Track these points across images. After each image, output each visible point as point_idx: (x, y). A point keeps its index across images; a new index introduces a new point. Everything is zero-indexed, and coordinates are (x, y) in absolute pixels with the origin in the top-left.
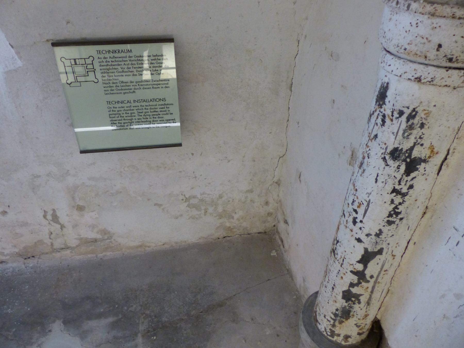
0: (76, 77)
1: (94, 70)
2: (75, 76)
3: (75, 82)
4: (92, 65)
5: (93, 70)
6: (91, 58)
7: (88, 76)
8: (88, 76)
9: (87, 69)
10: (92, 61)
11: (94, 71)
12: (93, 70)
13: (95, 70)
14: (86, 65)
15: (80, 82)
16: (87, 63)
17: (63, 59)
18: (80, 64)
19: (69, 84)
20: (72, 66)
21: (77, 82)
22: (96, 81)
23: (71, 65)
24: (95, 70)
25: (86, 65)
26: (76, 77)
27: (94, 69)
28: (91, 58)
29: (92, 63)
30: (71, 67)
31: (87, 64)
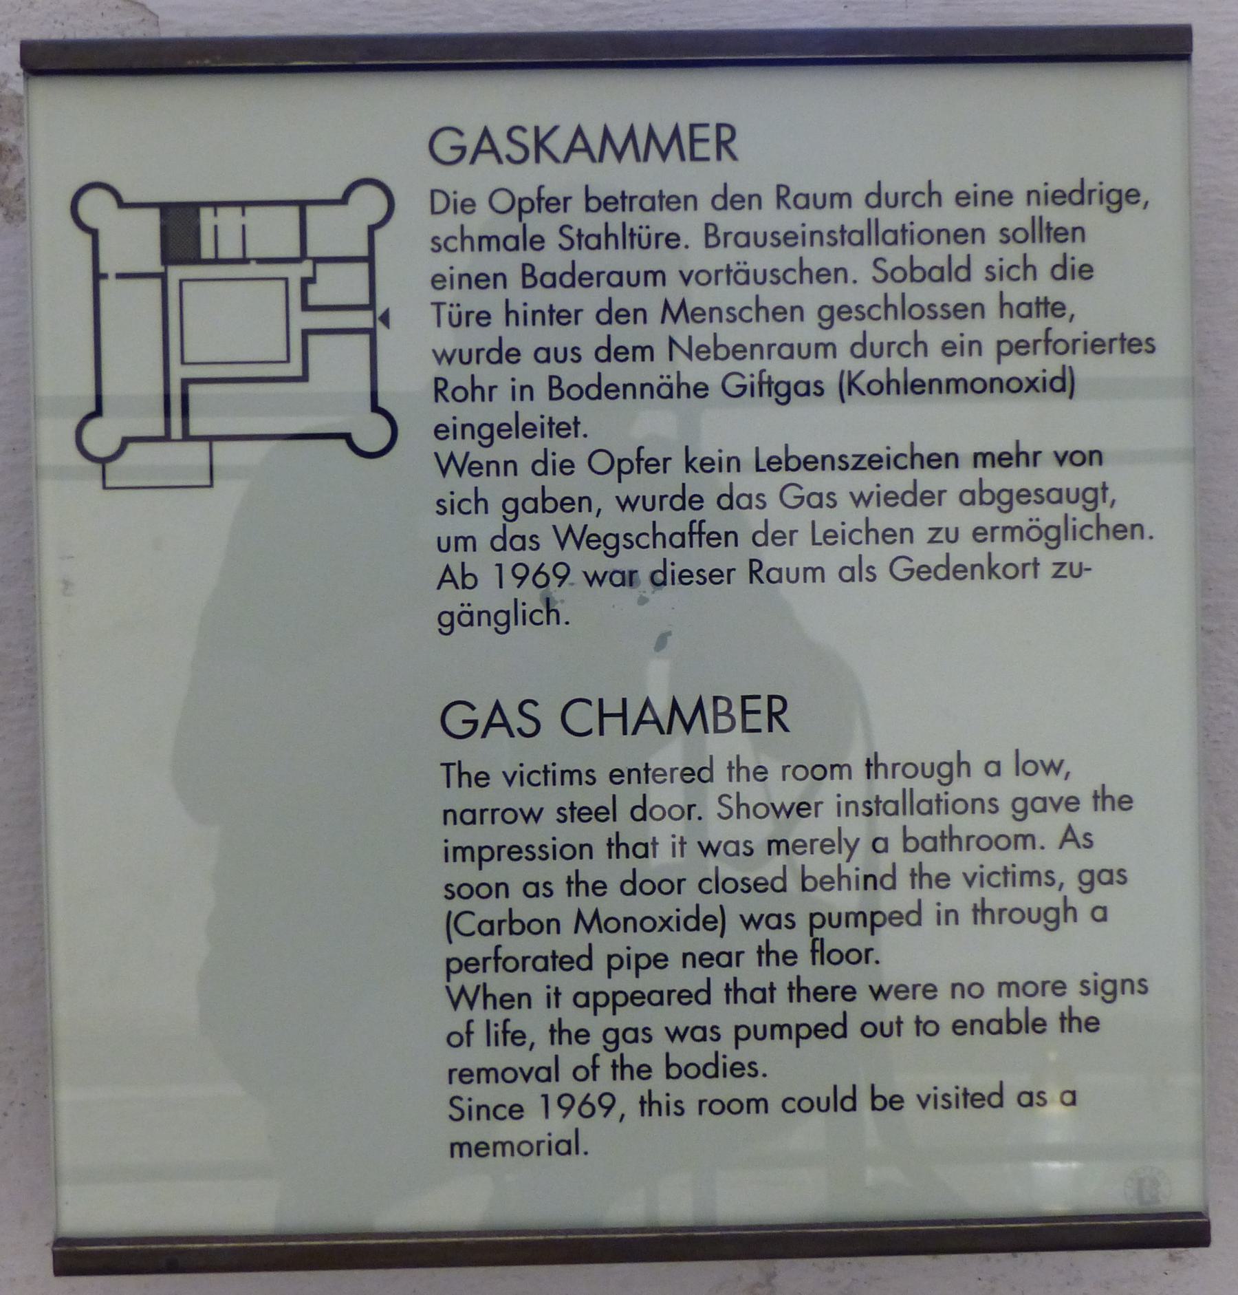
0: (185, 383)
1: (369, 325)
2: (178, 372)
3: (167, 438)
4: (364, 267)
5: (363, 319)
6: (369, 204)
7: (304, 378)
8: (304, 378)
9: (306, 307)
10: (372, 229)
11: (372, 332)
12: (363, 319)
13: (385, 319)
14: (305, 269)
15: (211, 439)
16: (312, 252)
17: (96, 208)
18: (244, 261)
19: (103, 461)
20: (163, 277)
21: (187, 437)
22: (373, 434)
23: (161, 269)
24: (380, 325)
25: (305, 269)
26: (185, 383)
27: (371, 306)
28: (369, 204)
29: (363, 251)
30: (157, 283)
31: (317, 260)
